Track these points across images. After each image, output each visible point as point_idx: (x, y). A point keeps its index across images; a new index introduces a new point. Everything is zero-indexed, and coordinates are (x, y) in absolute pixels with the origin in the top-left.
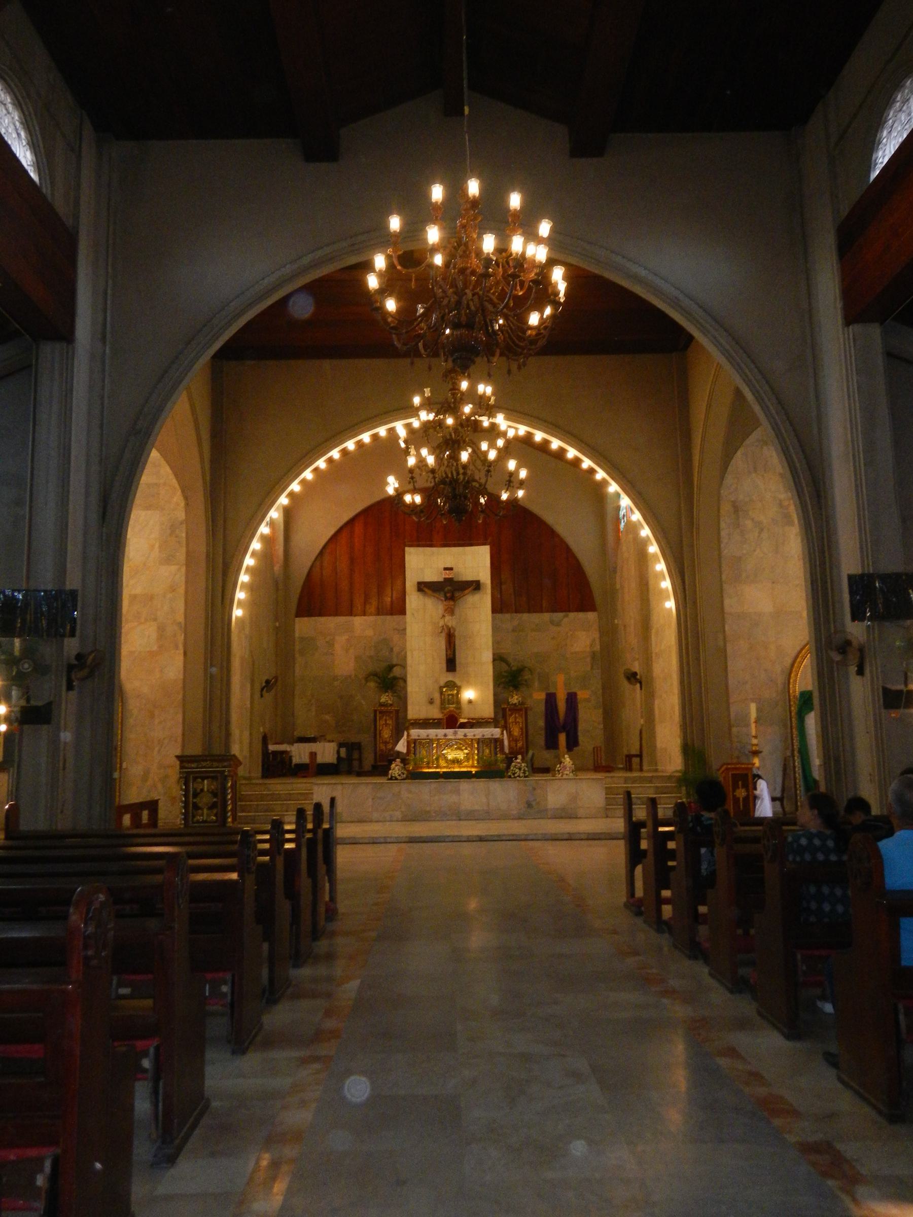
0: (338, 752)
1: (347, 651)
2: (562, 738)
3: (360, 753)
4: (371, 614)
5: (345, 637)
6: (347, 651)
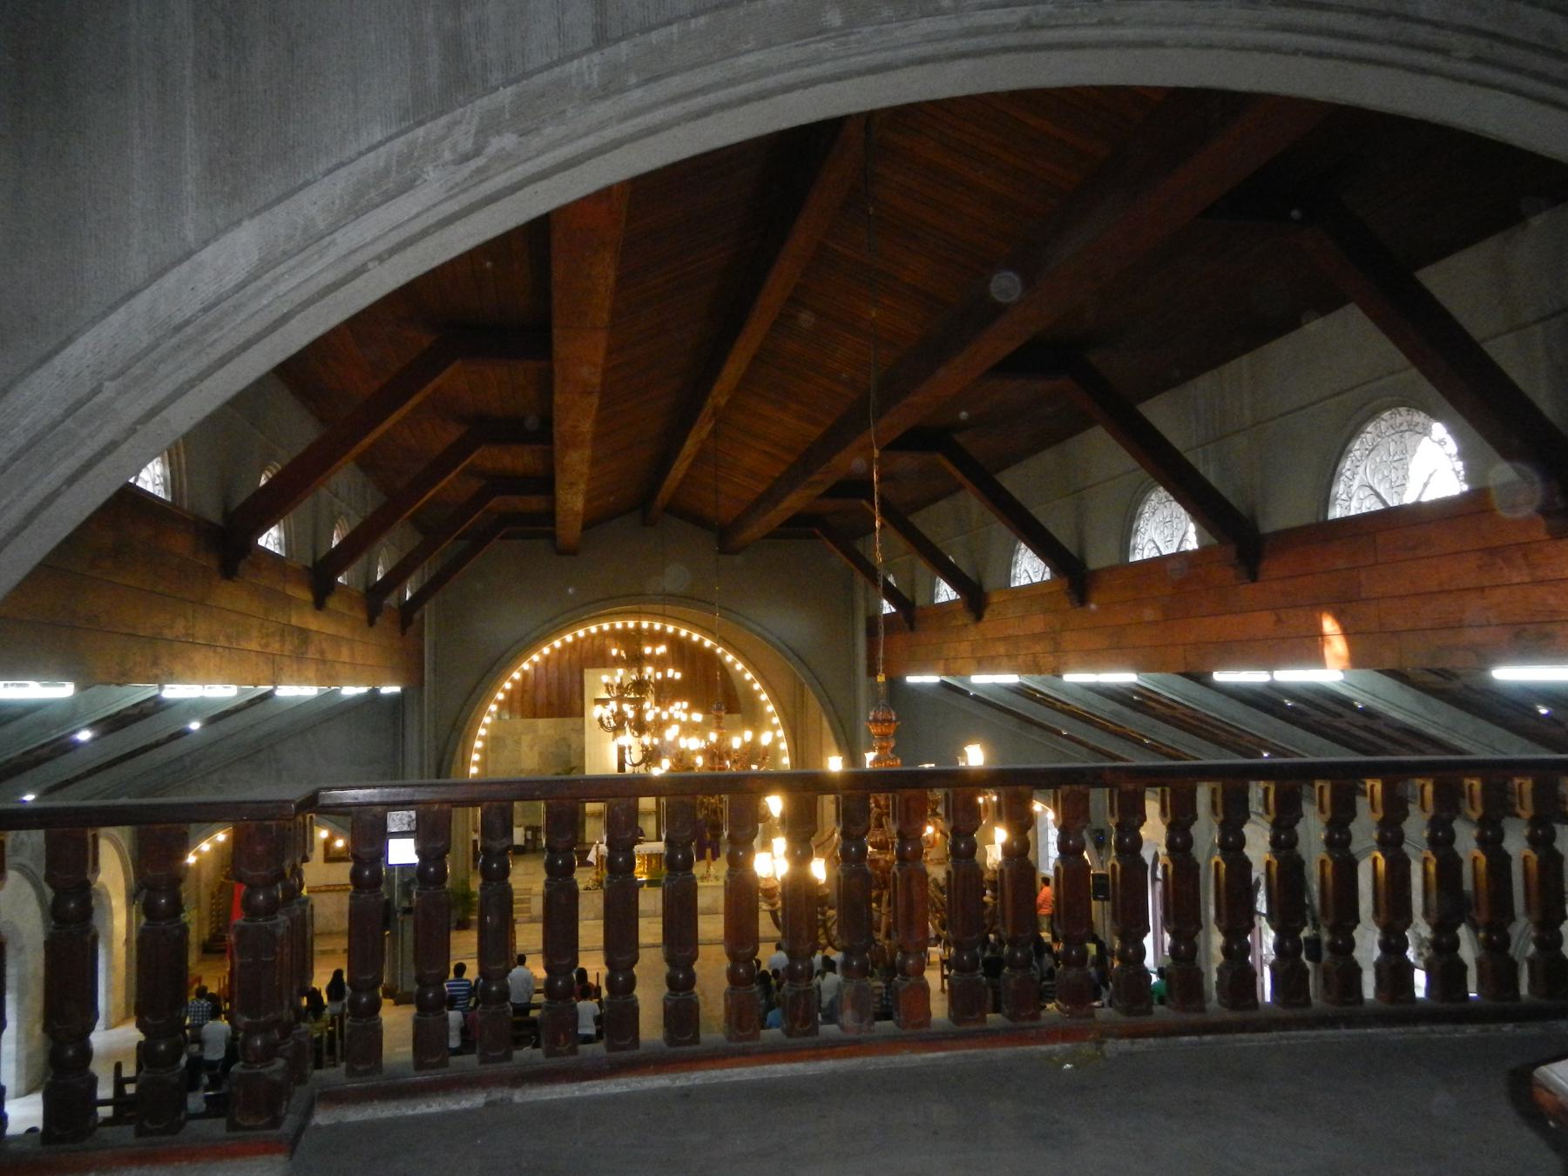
0: (525, 836)
1: (532, 748)
2: (709, 851)
4: (552, 717)
6: (532, 748)
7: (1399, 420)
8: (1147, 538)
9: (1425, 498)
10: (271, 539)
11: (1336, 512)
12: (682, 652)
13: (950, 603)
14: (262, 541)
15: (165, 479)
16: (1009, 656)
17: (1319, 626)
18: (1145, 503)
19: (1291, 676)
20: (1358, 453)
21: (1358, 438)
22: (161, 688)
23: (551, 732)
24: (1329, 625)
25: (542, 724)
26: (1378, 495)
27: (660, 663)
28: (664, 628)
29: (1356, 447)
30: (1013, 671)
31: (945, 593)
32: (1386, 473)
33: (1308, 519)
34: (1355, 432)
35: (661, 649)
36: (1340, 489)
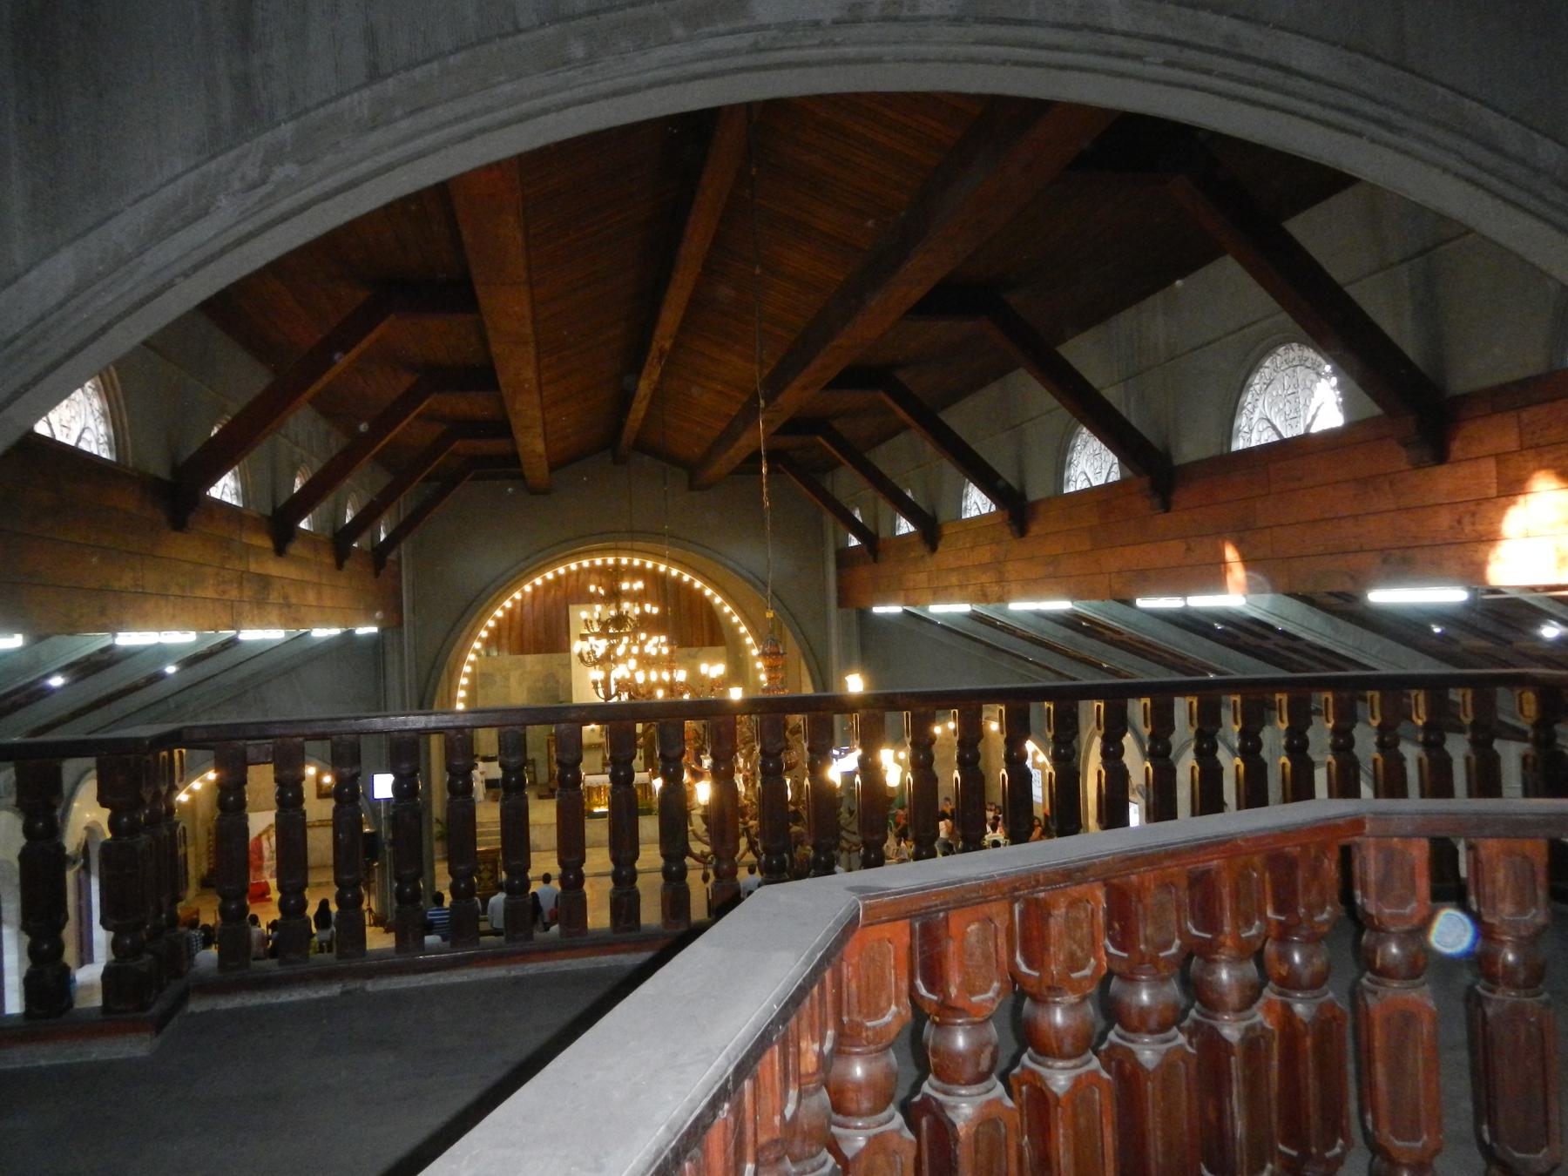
3: (534, 767)
5: (519, 672)
7: (1292, 354)
8: (1079, 469)
9: (1314, 430)
10: (225, 489)
11: (1239, 444)
12: (660, 587)
13: (909, 534)
14: (215, 492)
15: (109, 438)
16: (961, 586)
17: (1221, 554)
18: (1078, 436)
19: (1200, 602)
20: (1257, 387)
21: (1257, 372)
22: (114, 636)
23: (539, 667)
24: (1231, 554)
25: (530, 659)
26: (1274, 428)
27: (638, 598)
28: (643, 565)
29: (1256, 381)
30: (964, 600)
31: (905, 527)
32: (1281, 407)
33: (1213, 451)
34: (1254, 367)
35: (639, 585)
36: (1242, 422)
